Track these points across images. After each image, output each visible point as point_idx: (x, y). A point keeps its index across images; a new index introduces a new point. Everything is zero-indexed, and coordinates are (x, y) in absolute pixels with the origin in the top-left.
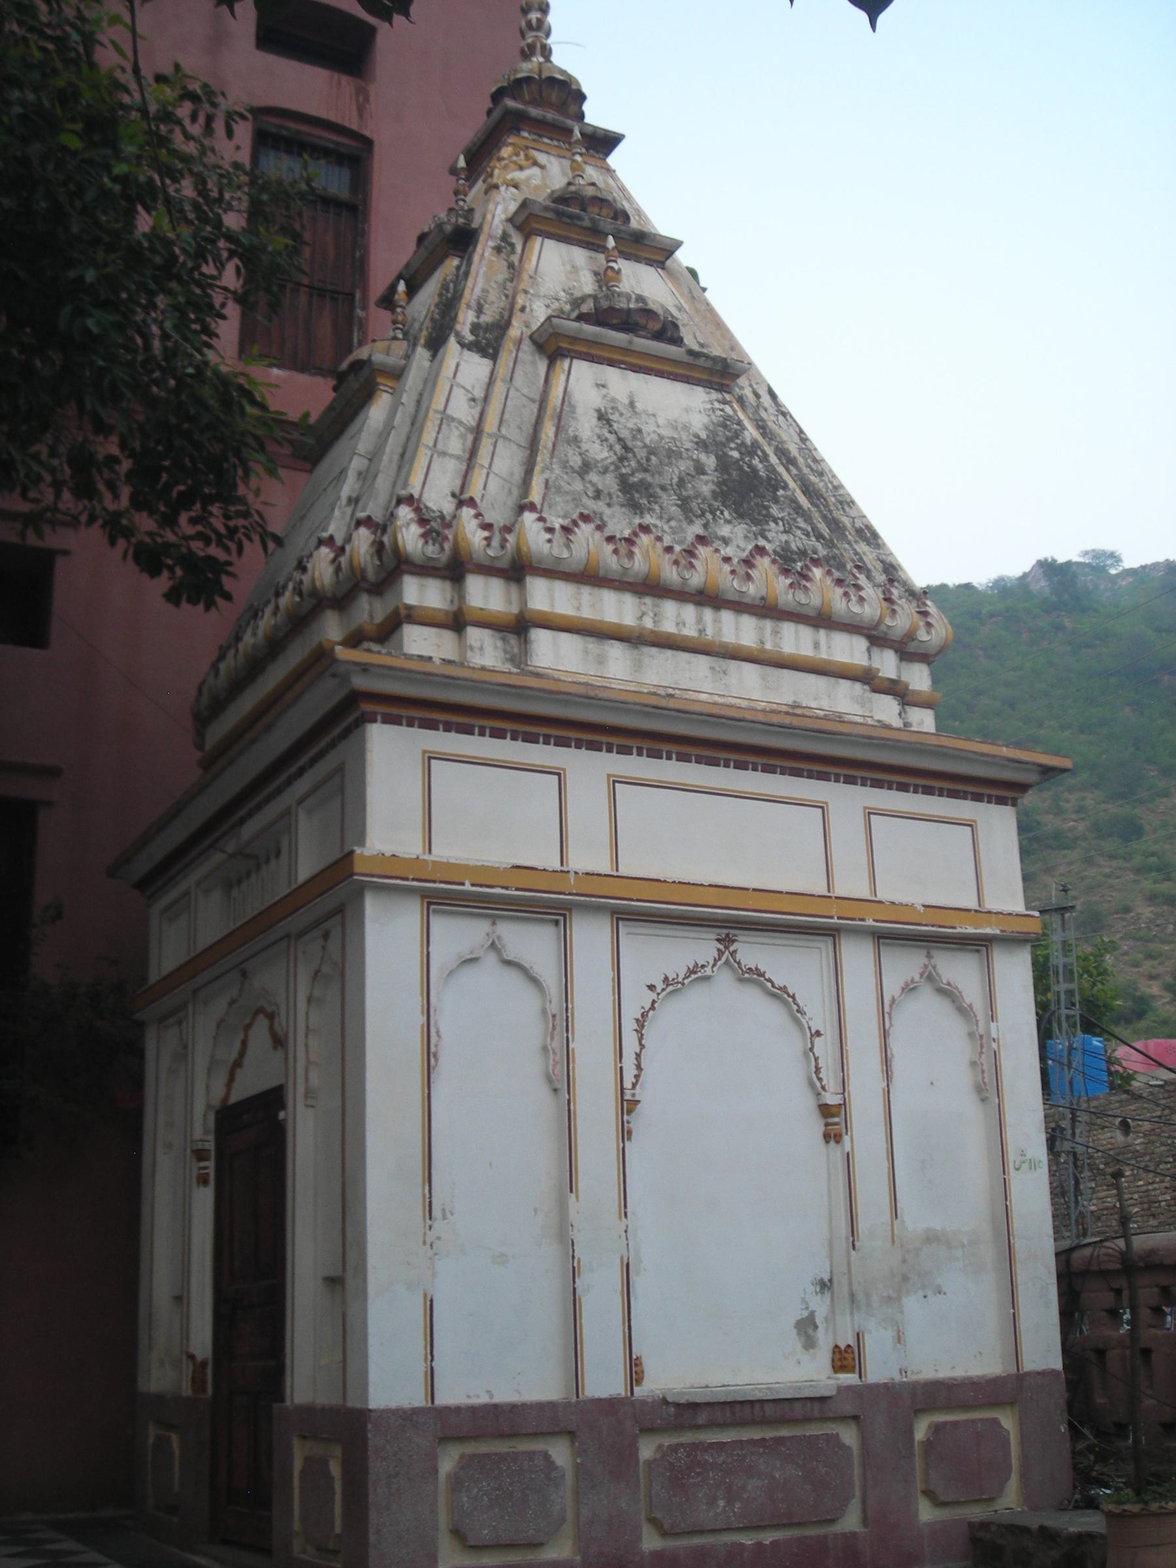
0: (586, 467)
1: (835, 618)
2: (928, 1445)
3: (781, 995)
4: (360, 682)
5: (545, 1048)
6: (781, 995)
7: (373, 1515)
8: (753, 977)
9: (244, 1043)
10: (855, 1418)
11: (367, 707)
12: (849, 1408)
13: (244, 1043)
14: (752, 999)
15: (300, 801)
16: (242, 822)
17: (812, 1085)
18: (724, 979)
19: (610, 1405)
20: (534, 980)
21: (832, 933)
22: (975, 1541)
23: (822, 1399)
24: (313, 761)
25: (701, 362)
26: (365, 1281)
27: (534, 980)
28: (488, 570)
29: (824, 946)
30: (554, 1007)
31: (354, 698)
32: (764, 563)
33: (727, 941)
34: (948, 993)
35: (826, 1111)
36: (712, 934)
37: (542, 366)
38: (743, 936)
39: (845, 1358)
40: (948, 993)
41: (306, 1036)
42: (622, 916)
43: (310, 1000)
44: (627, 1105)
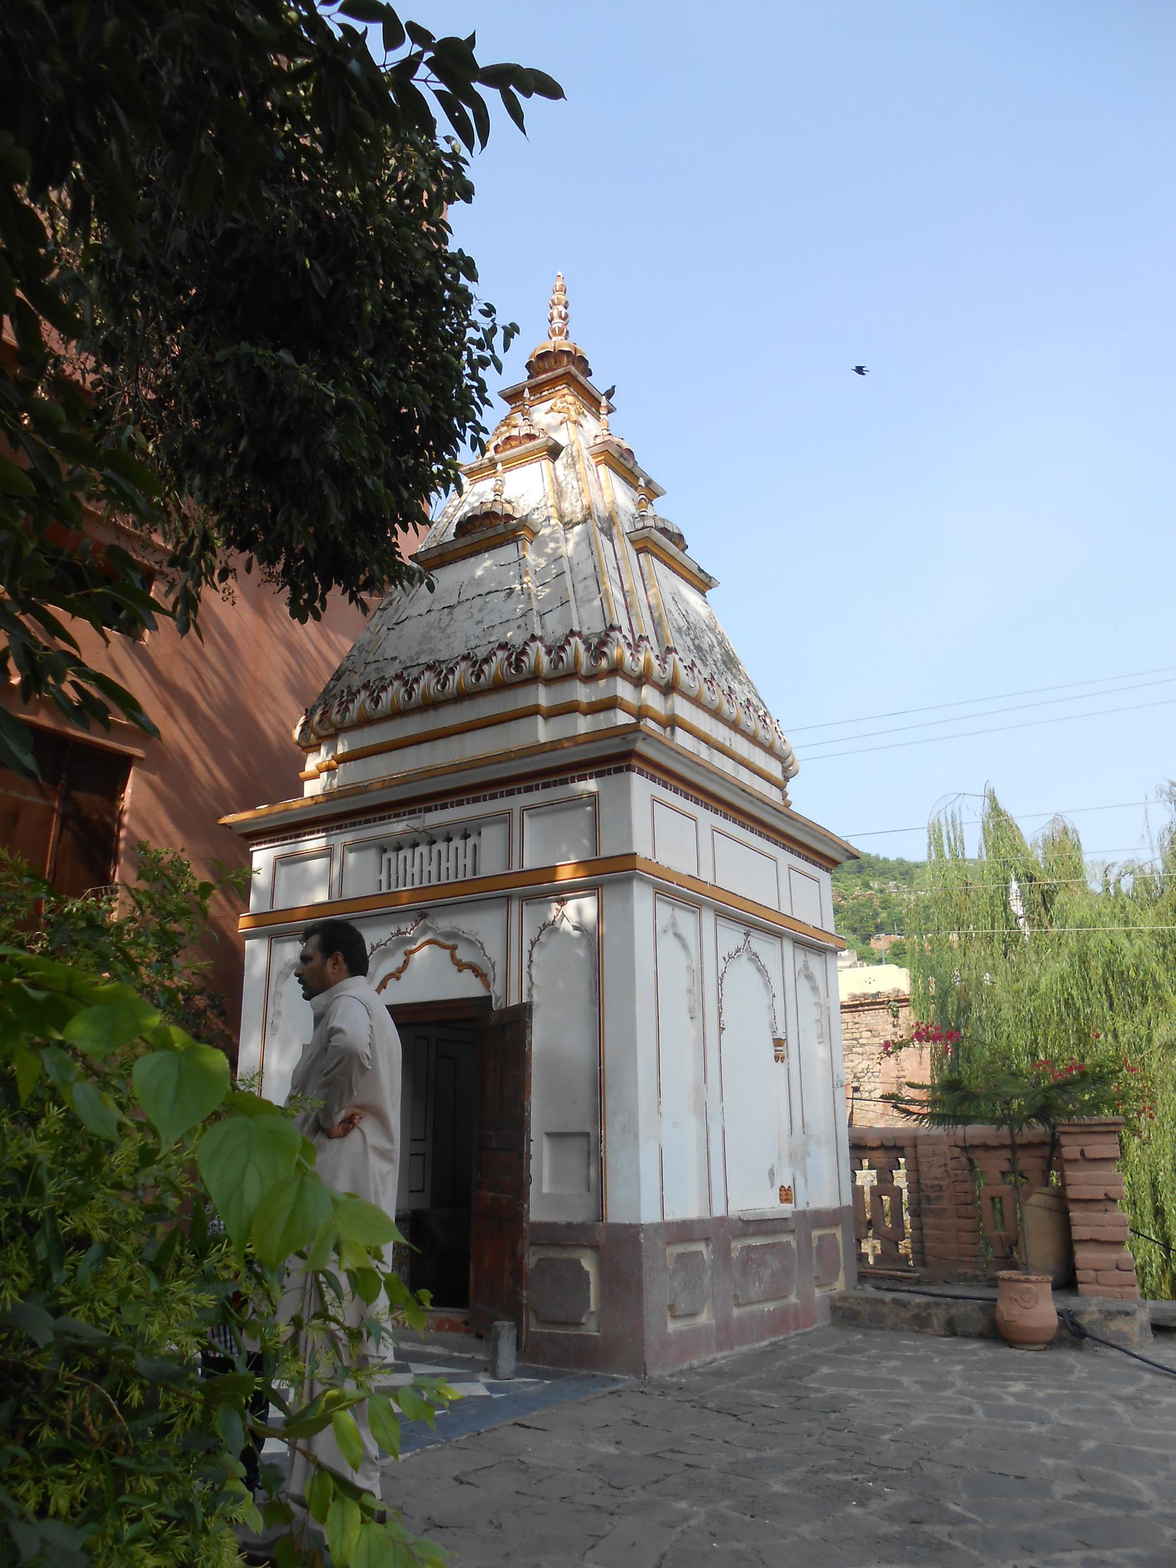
0: (679, 630)
1: (775, 750)
2: (819, 1248)
3: (762, 970)
4: (642, 747)
5: (689, 991)
6: (762, 970)
7: (646, 1298)
8: (754, 957)
9: (406, 962)
10: (793, 1231)
11: (634, 762)
12: (792, 1225)
13: (406, 962)
14: (751, 968)
15: (524, 809)
16: (428, 810)
17: (771, 1026)
18: (744, 957)
19: (722, 1220)
20: (685, 947)
21: (779, 935)
22: (834, 1309)
23: (785, 1219)
24: (546, 786)
25: (701, 576)
26: (636, 1136)
27: (685, 947)
28: (656, 685)
29: (777, 942)
30: (695, 965)
31: (630, 754)
32: (751, 709)
33: (747, 934)
34: (809, 977)
35: (778, 1042)
36: (743, 929)
37: (632, 553)
38: (754, 933)
39: (786, 1195)
40: (809, 977)
41: (529, 967)
42: (720, 914)
43: (533, 944)
44: (722, 1029)
